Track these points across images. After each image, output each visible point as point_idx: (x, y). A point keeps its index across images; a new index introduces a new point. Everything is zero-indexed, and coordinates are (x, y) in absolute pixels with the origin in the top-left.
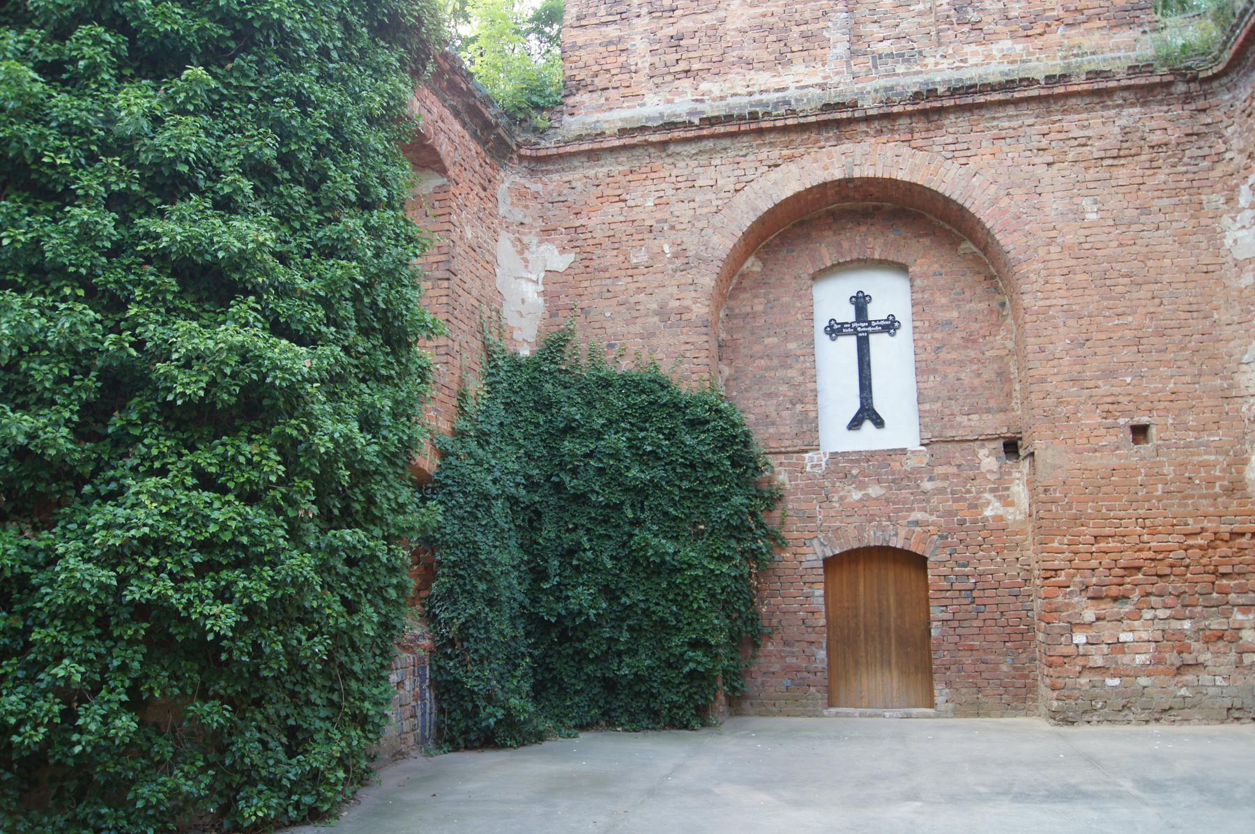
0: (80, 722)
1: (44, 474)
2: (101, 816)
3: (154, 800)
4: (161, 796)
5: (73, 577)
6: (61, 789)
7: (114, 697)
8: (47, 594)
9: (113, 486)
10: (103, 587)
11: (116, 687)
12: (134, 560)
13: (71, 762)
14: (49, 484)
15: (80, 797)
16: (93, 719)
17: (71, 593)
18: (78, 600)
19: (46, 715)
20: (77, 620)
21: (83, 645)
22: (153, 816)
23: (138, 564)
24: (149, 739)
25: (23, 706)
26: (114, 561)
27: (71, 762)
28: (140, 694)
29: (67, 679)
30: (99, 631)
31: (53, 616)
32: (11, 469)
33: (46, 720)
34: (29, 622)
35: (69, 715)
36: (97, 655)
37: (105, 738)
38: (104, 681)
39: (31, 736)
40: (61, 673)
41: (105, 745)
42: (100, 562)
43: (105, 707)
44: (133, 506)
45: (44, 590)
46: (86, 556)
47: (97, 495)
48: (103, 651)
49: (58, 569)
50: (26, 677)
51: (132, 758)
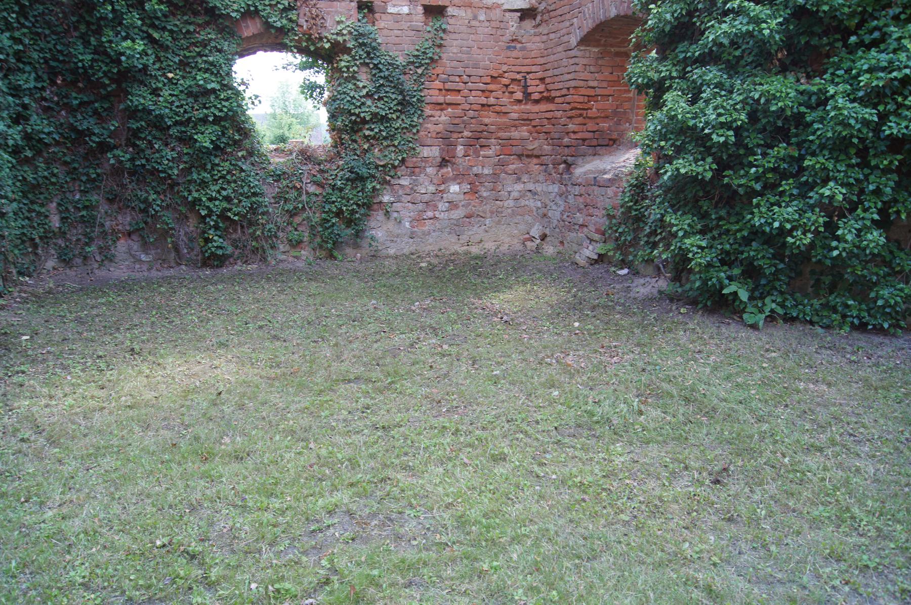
0: (839, 232)
1: (818, 29)
2: (847, 306)
3: (892, 302)
4: (898, 299)
5: (841, 114)
6: (818, 281)
7: (867, 215)
8: (818, 129)
9: (876, 34)
10: (866, 123)
11: (870, 207)
12: (894, 99)
13: (828, 262)
14: (820, 38)
15: (832, 289)
16: (850, 231)
17: (839, 128)
18: (844, 133)
19: (813, 224)
20: (840, 150)
21: (845, 171)
22: (889, 314)
23: (897, 103)
24: (891, 252)
25: (796, 217)
26: (876, 101)
27: (828, 262)
28: (889, 215)
29: (832, 198)
30: (859, 160)
31: (822, 147)
32: (791, 27)
33: (813, 228)
34: (803, 152)
35: (831, 227)
36: (856, 180)
37: (858, 247)
38: (861, 202)
39: (801, 239)
40: (827, 193)
41: (858, 252)
42: (862, 101)
43: (860, 223)
44: (895, 51)
45: (816, 126)
46: (852, 97)
47: (861, 44)
48: (861, 177)
49: (828, 108)
50: (799, 195)
51: (876, 266)
